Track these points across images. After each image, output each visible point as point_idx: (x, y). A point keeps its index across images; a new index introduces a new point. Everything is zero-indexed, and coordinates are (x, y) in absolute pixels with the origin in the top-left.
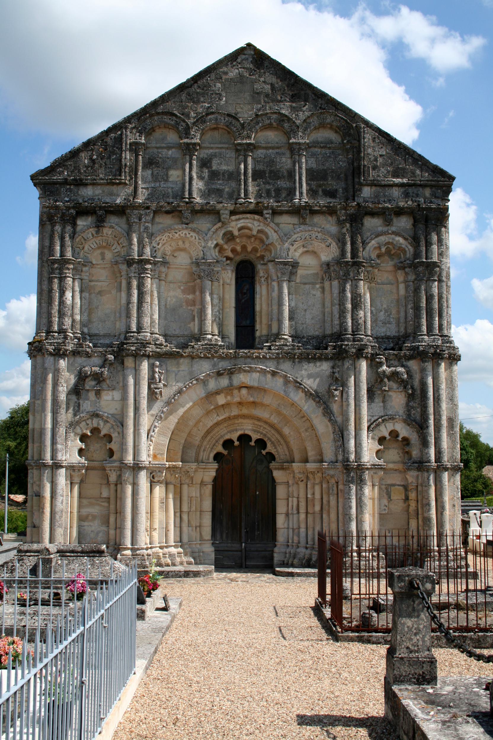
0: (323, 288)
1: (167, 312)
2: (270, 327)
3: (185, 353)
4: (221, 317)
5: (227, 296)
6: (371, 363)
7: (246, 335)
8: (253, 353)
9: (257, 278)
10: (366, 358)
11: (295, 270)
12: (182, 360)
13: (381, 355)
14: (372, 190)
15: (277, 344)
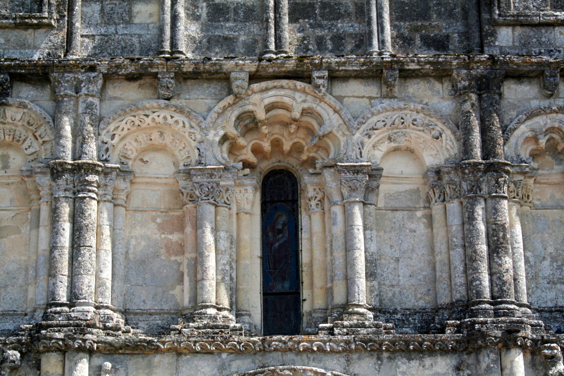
0: (430, 219)
1: (128, 266)
2: (329, 292)
3: (163, 343)
4: (234, 275)
5: (245, 237)
6: (532, 358)
7: (283, 308)
8: (299, 342)
9: (302, 202)
10: (523, 347)
11: (375, 183)
12: (157, 358)
13: (552, 342)
14: (516, 33)
15: (346, 323)
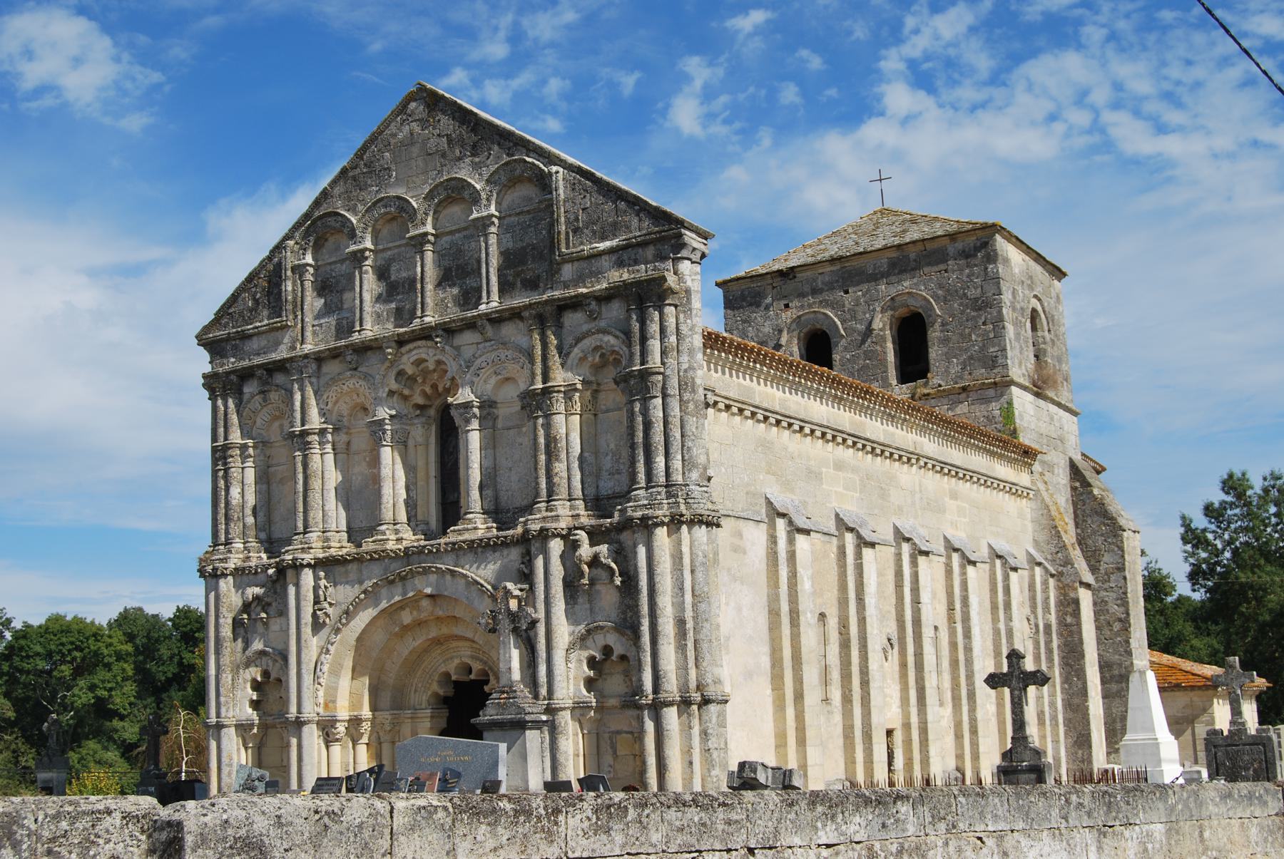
12: (350, 566)
